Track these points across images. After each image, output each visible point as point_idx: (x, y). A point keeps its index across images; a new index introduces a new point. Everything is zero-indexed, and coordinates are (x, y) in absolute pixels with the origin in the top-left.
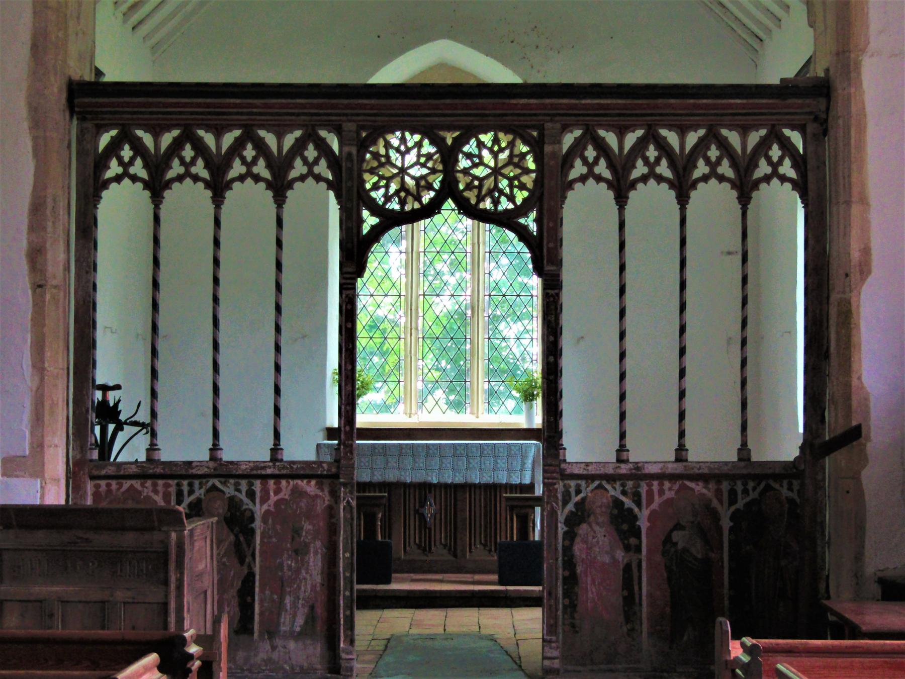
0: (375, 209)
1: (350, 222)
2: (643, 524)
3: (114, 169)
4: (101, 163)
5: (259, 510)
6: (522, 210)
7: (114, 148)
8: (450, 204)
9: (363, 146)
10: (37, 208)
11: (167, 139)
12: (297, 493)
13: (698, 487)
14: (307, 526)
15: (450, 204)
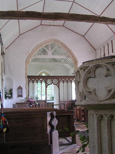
0: (48, 84)
1: (46, 85)
2: (65, 104)
3: (30, 81)
4: (29, 81)
5: (40, 104)
6: (57, 84)
7: (30, 80)
8: (52, 84)
9: (47, 80)
10: (26, 84)
11: (34, 79)
12: (43, 103)
13: (69, 102)
14: (43, 105)
15: (52, 84)
